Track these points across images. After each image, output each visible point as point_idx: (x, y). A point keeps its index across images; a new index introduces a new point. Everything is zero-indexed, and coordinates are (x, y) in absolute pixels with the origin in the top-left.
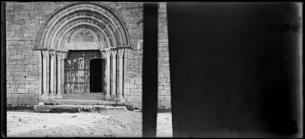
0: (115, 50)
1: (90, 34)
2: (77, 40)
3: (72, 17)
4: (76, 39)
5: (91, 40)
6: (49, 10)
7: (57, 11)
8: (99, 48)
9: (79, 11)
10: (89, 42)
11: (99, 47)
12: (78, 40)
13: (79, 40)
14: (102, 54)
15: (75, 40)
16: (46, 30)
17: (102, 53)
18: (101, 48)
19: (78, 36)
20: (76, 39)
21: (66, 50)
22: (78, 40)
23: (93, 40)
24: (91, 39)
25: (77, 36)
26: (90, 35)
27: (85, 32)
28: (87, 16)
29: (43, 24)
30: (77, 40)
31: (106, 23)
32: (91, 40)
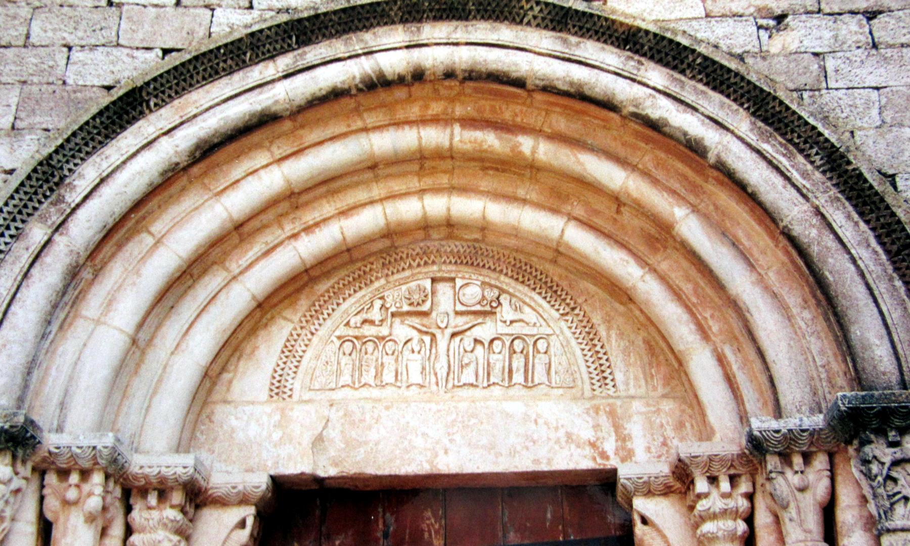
0: (807, 458)
1: (506, 312)
2: (369, 377)
3: (332, 139)
4: (359, 369)
5: (518, 377)
6: (99, 54)
7: (174, 60)
8: (604, 455)
9: (400, 80)
10: (497, 391)
11: (610, 446)
12: (378, 374)
13: (388, 377)
14: (645, 521)
15: (346, 379)
16: (37, 233)
17: (640, 504)
18: (627, 455)
19: (384, 331)
20: (359, 369)
21: (250, 470)
22: (378, 374)
23: (539, 375)
24: (518, 362)
25: (369, 330)
26: (502, 329)
27: (456, 298)
28: (478, 135)
29: (11, 172)
30: (369, 377)
31: (673, 192)
32: (518, 377)
